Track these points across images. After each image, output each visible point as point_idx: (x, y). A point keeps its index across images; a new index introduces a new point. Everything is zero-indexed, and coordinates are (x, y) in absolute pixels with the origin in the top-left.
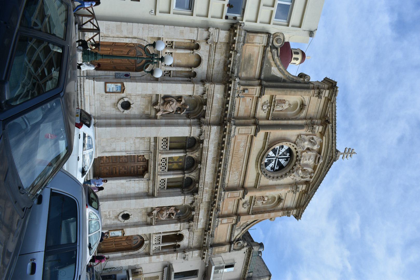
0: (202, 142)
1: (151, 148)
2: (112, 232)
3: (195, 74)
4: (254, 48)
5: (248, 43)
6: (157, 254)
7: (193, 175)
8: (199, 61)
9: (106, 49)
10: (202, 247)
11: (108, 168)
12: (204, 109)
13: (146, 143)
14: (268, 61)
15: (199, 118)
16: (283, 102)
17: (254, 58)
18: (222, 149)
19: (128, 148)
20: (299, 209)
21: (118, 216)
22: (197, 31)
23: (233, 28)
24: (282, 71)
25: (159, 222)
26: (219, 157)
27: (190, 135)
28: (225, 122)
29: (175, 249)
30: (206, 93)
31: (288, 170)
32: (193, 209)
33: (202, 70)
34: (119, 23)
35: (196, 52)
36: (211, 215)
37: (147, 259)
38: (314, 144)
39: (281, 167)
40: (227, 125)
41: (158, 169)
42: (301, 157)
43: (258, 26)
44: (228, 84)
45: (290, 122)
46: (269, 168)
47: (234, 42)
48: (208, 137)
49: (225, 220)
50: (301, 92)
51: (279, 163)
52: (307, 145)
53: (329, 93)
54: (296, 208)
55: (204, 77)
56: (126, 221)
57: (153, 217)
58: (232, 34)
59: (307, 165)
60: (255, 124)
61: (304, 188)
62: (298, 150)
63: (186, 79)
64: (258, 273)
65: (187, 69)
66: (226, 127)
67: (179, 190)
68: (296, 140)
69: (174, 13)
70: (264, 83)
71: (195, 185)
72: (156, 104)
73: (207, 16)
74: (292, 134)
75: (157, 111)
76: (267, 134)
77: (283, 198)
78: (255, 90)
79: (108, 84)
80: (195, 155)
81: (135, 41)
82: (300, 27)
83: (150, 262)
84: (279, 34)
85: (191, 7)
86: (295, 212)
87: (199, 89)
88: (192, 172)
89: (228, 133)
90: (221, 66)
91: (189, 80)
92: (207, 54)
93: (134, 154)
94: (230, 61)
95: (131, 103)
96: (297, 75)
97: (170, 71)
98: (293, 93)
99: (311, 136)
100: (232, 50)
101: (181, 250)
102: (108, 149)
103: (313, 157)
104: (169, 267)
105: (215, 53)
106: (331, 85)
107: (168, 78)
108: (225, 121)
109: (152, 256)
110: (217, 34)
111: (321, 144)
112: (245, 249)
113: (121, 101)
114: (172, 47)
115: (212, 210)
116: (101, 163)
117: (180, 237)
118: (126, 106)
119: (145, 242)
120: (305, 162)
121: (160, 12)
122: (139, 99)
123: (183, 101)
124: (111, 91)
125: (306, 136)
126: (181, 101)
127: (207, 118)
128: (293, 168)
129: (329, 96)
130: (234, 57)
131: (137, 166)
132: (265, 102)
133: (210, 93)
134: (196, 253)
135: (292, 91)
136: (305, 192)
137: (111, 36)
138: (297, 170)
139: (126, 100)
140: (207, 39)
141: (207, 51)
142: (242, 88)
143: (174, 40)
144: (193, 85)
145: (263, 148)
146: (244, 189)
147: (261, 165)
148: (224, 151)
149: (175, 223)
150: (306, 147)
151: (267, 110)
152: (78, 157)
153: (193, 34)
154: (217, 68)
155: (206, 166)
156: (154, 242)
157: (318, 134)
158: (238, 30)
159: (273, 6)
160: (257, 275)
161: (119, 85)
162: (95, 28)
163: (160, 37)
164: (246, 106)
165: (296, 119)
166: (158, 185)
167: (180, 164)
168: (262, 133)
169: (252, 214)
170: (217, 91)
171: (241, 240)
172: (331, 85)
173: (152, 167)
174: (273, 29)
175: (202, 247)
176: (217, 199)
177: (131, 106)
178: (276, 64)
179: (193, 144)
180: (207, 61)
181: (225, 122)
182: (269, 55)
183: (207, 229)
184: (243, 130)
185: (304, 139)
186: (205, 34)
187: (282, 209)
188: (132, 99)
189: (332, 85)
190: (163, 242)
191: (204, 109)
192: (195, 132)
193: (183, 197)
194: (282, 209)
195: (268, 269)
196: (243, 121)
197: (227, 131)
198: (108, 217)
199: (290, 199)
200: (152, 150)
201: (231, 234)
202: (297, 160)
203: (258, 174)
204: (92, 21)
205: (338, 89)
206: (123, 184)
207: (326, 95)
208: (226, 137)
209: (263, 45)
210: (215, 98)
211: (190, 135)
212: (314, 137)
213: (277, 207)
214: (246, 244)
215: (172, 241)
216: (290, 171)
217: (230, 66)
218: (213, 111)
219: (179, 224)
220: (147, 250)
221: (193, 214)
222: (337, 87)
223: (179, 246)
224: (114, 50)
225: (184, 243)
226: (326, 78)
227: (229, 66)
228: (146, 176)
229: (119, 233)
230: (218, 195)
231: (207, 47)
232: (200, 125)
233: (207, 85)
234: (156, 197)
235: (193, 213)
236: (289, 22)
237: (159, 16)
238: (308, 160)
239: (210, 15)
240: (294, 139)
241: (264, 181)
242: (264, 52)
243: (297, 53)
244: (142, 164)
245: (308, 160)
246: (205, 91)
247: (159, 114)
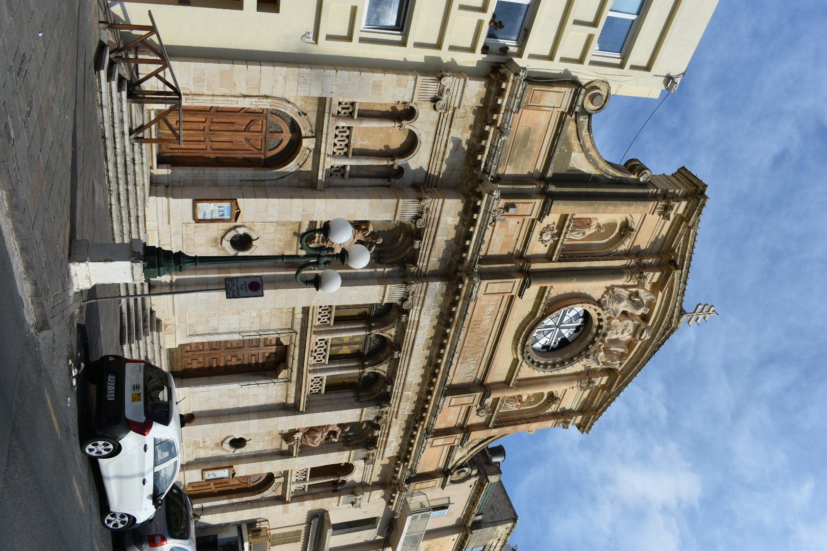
0: (407, 312)
1: (295, 324)
2: (210, 472)
5: (527, 107)
6: (299, 497)
7: (383, 369)
8: (412, 143)
9: (196, 119)
10: (388, 484)
11: (201, 359)
12: (416, 247)
13: (284, 315)
14: (567, 139)
17: (536, 137)
18: (449, 325)
19: (246, 326)
20: (589, 413)
21: (222, 442)
22: (413, 82)
23: (496, 71)
24: (594, 160)
25: (305, 451)
26: (439, 340)
27: (382, 301)
28: (459, 274)
29: (335, 489)
30: (424, 216)
31: (577, 351)
32: (378, 427)
34: (226, 67)
35: (407, 125)
36: (413, 437)
37: (280, 508)
38: (638, 306)
40: (463, 283)
41: (309, 360)
42: (608, 329)
43: (555, 67)
44: (473, 199)
47: (496, 109)
48: (421, 302)
49: (440, 441)
50: (629, 205)
52: (624, 306)
53: (686, 207)
54: (581, 411)
56: (238, 451)
57: (291, 443)
58: (494, 89)
59: (616, 342)
61: (603, 382)
62: (604, 317)
63: (380, 181)
64: (491, 513)
65: (384, 163)
66: (460, 286)
67: (351, 394)
68: (603, 297)
69: (362, 40)
70: (552, 188)
71: (386, 388)
73: (438, 46)
74: (595, 288)
76: (542, 291)
78: (531, 206)
79: (200, 205)
80: (390, 333)
81: (265, 104)
82: (648, 68)
83: (285, 511)
84: (598, 85)
85: (403, 24)
86: (579, 419)
87: (408, 208)
88: (380, 362)
89: (465, 298)
91: (389, 183)
92: (433, 129)
93: (258, 337)
94: (483, 148)
95: (254, 236)
96: (623, 164)
97: (344, 167)
98: (611, 208)
99: (634, 290)
100: (491, 125)
101: (347, 488)
102: (200, 330)
103: (631, 328)
104: (323, 515)
105: (450, 127)
106: (692, 189)
107: (338, 181)
108: (460, 271)
109: (288, 502)
110: (460, 88)
111: (651, 305)
112: (472, 481)
113: (232, 234)
114: (351, 115)
115: (416, 429)
116: (187, 351)
117: (348, 468)
118: (243, 242)
119: (277, 481)
120: (614, 337)
121: (329, 37)
122: (271, 228)
123: (371, 229)
124: (208, 217)
125: (623, 290)
126: (367, 229)
127: (420, 264)
128: (587, 349)
129: (684, 212)
130: (494, 138)
131: (264, 353)
132: (548, 226)
133: (434, 215)
134: (378, 494)
135: (609, 205)
136: (607, 387)
137: (206, 92)
138: (595, 352)
139: (241, 231)
140: (435, 100)
141: (432, 124)
142: (503, 202)
143: (357, 100)
144: (395, 200)
145: (533, 314)
147: (523, 346)
148: (451, 331)
149: (339, 450)
151: (551, 241)
152: (145, 446)
153: (403, 89)
155: (410, 355)
156: (294, 479)
157: (648, 287)
158: (510, 84)
159: (594, 24)
160: (491, 517)
161: (226, 205)
162: (169, 89)
163: (324, 96)
164: (506, 236)
166: (307, 389)
167: (357, 347)
168: (533, 290)
169: (495, 427)
171: (466, 466)
172: (692, 189)
173: (296, 358)
174: (584, 73)
175: (388, 484)
176: (429, 414)
177: (254, 243)
178: (582, 146)
180: (431, 145)
181: (459, 274)
182: (571, 127)
183: (403, 455)
184: (497, 286)
185: (618, 295)
186: (432, 88)
187: (554, 415)
188: (256, 229)
189: (696, 191)
191: (416, 247)
192: (393, 293)
193: (358, 411)
194: (554, 415)
195: (511, 506)
197: (463, 295)
198: (201, 445)
199: (571, 396)
200: (297, 328)
201: (449, 457)
202: (597, 334)
203: (515, 362)
204: (161, 74)
205: (708, 203)
206: (233, 390)
207: (680, 211)
208: (460, 306)
209: (561, 110)
210: (441, 225)
211: (382, 301)
212: (641, 291)
213: (545, 411)
214: (475, 472)
215: (332, 480)
216: (580, 353)
219: (347, 453)
220: (279, 493)
221: (376, 434)
222: (706, 198)
223: (344, 482)
224: (215, 120)
226: (683, 168)
227: (479, 157)
228: (283, 374)
229: (224, 473)
230: (430, 407)
231: (435, 115)
234: (302, 413)
235: (376, 433)
236: (624, 58)
237: (326, 48)
238: (622, 332)
239: (445, 46)
240: (597, 296)
241: (526, 371)
242: (561, 123)
244: (273, 349)
245: (622, 332)
246: (422, 213)
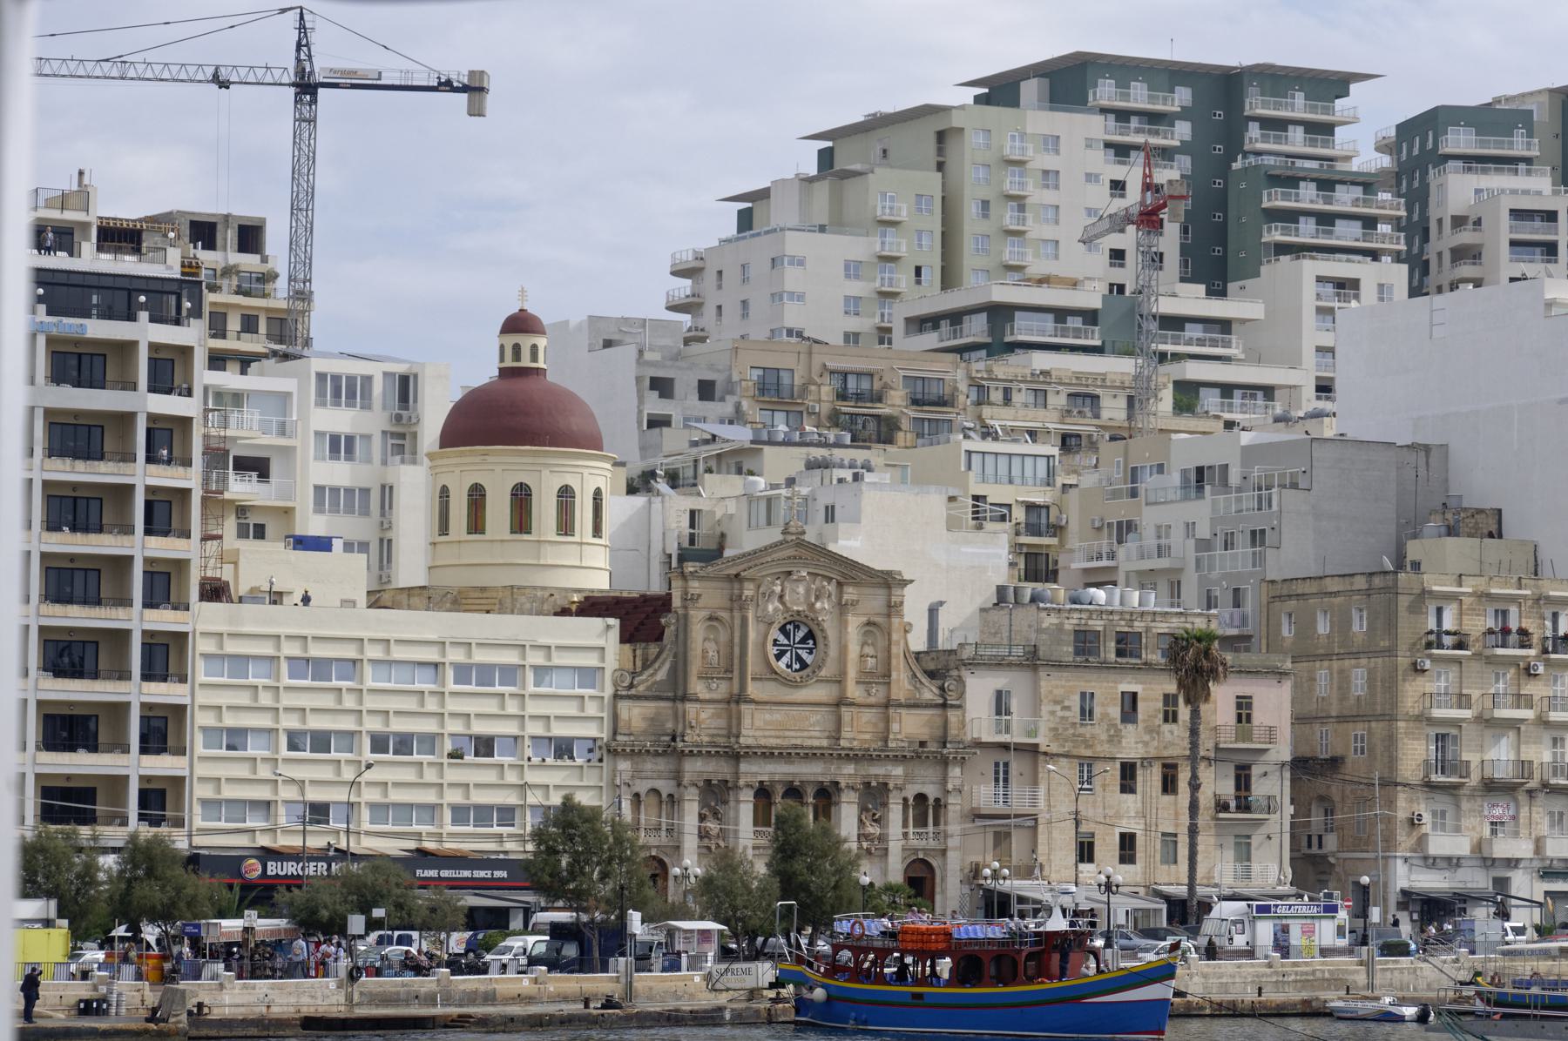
3: (671, 796)
4: (635, 714)
8: (655, 791)
14: (648, 689)
15: (729, 789)
16: (705, 652)
33: (665, 787)
39: (810, 635)
45: (737, 640)
46: (808, 658)
51: (803, 641)
55: (673, 783)
60: (738, 702)
72: (709, 848)
75: (718, 846)
77: (864, 619)
90: (660, 760)
146: (840, 703)
150: (777, 604)
154: (662, 765)
165: (732, 628)
170: (695, 768)
174: (609, 691)
179: (763, 793)
190: (925, 825)
192: (747, 796)
193: (844, 806)
196: (733, 731)
213: (879, 630)
217: (660, 750)
218: (717, 769)
223: (937, 800)
225: (932, 792)
232: (737, 787)
233: (686, 781)
235: (874, 784)
238: (797, 596)
243: (517, 349)
247: (722, 844)
